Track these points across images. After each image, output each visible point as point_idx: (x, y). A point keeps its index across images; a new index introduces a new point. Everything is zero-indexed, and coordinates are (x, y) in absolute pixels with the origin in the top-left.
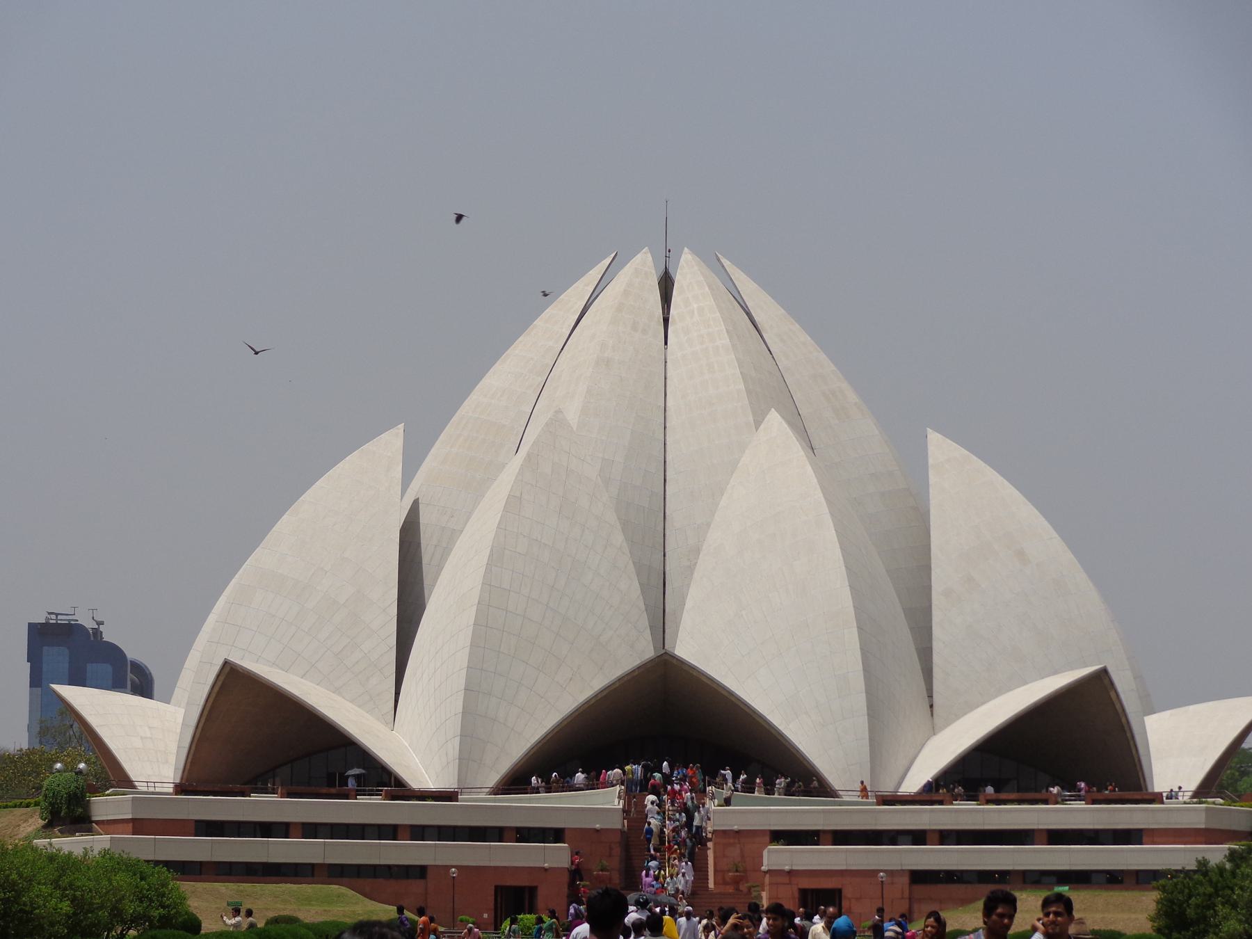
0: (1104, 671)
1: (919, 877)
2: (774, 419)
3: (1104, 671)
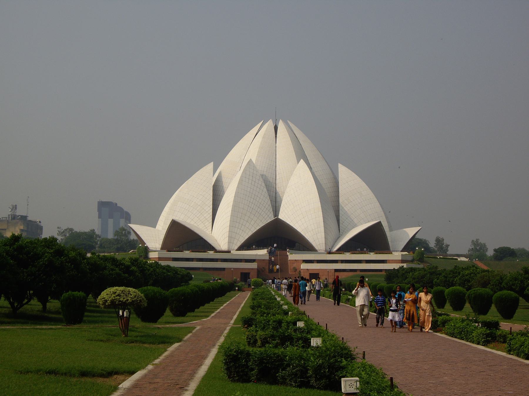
0: (380, 222)
1: (336, 270)
2: (302, 160)
3: (380, 222)
